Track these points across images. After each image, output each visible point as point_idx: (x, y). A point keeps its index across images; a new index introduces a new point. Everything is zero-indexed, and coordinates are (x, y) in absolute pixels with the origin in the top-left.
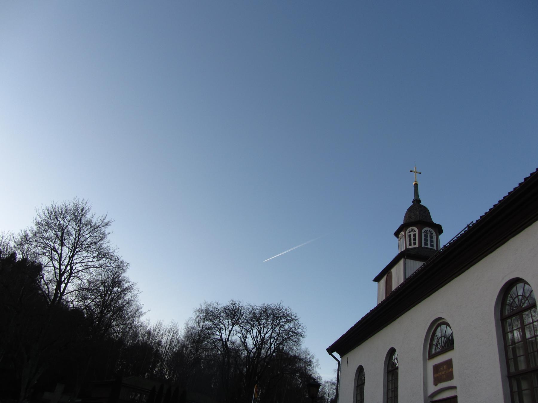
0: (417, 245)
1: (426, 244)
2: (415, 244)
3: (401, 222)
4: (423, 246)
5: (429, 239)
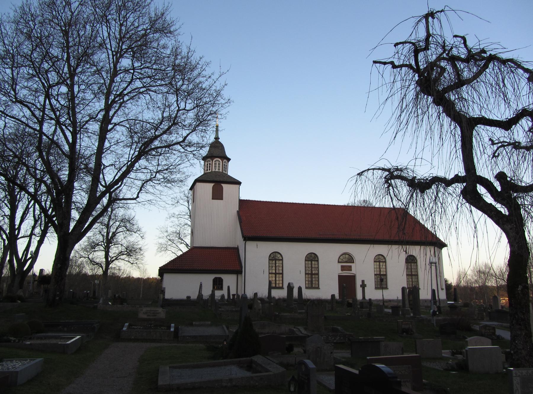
5: (217, 165)
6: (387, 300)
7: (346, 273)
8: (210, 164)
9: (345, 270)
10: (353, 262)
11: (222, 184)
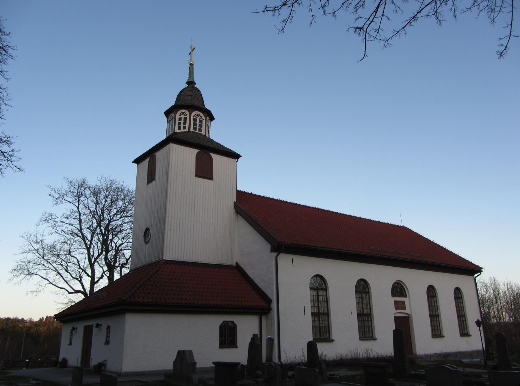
0: (187, 130)
1: (195, 129)
2: (185, 128)
3: (172, 103)
4: (192, 130)
6: (445, 353)
7: (400, 313)
8: (185, 119)
9: (399, 309)
10: (406, 296)
11: (211, 154)
